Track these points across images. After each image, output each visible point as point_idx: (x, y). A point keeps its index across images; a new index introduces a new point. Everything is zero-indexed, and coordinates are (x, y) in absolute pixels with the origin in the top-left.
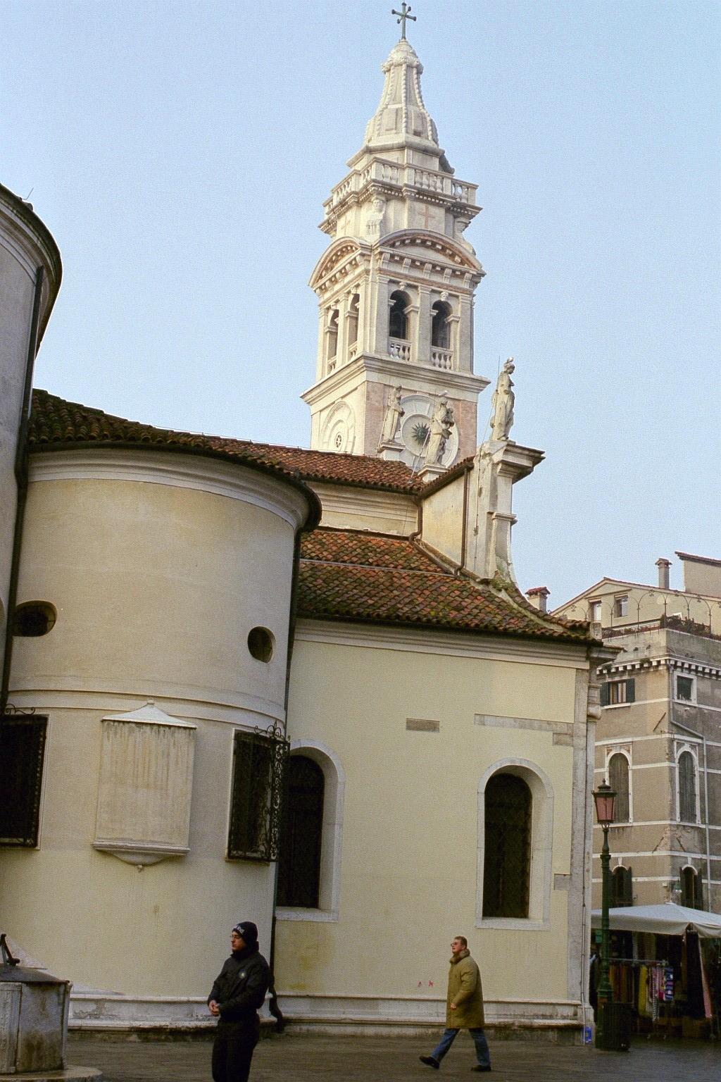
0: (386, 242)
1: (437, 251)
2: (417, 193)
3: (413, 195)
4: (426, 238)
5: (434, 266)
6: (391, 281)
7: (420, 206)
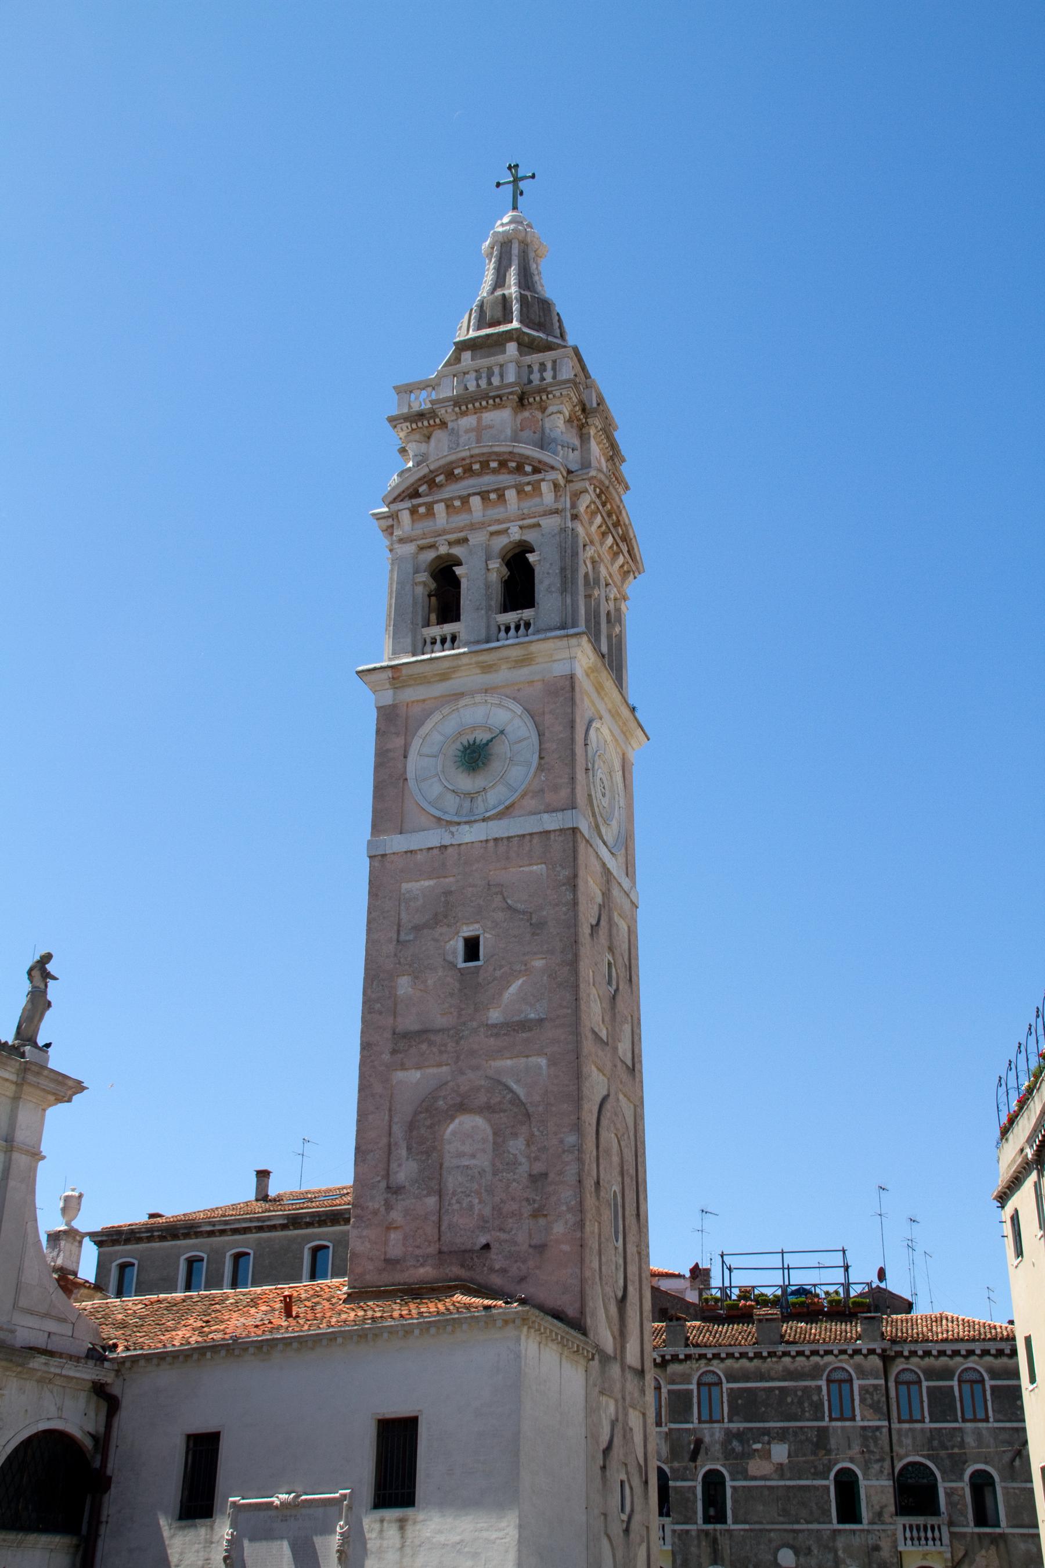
0: (399, 495)
1: (495, 471)
2: (455, 406)
3: (449, 410)
4: (468, 461)
5: (484, 495)
6: (422, 548)
7: (469, 421)
